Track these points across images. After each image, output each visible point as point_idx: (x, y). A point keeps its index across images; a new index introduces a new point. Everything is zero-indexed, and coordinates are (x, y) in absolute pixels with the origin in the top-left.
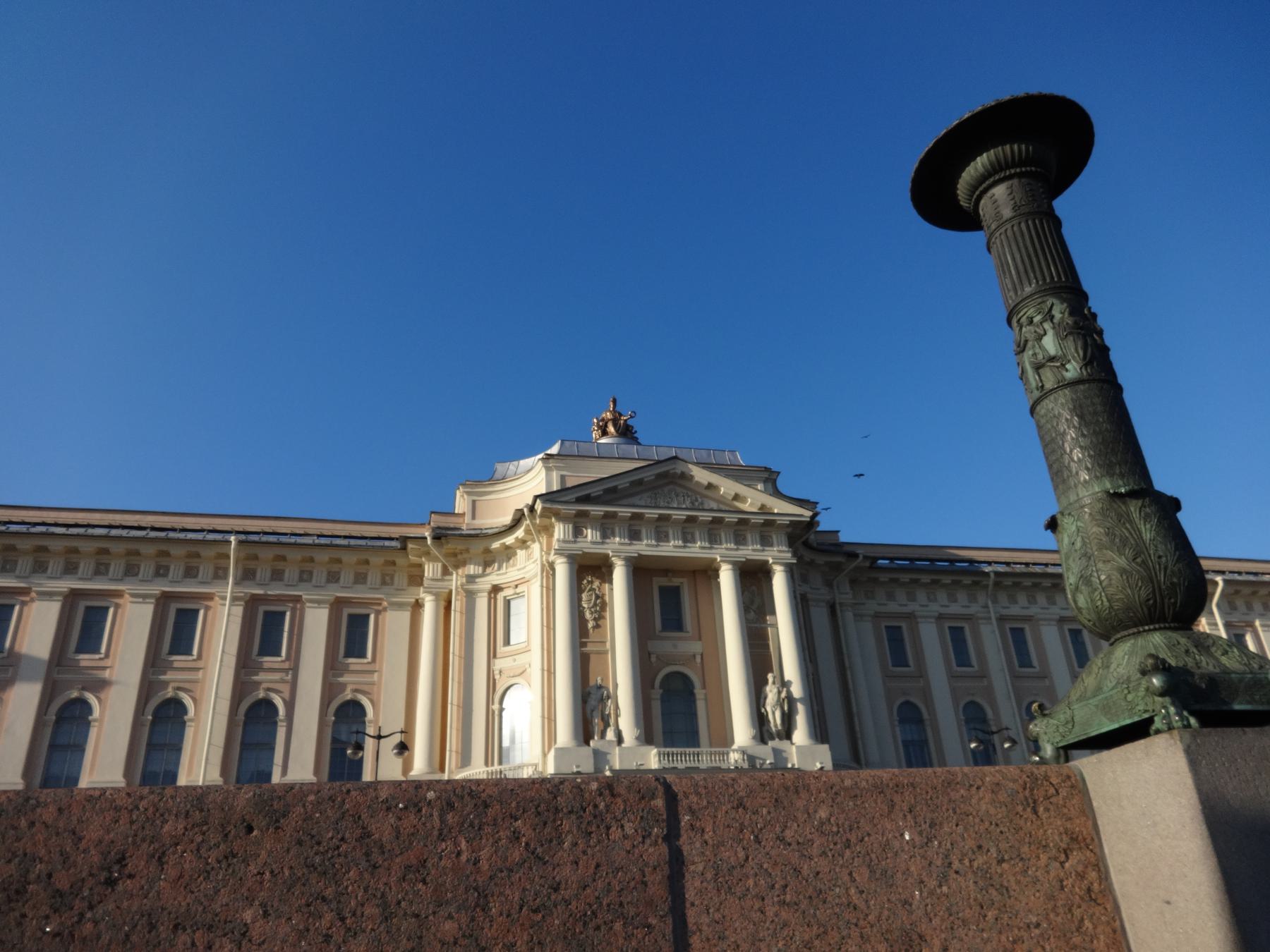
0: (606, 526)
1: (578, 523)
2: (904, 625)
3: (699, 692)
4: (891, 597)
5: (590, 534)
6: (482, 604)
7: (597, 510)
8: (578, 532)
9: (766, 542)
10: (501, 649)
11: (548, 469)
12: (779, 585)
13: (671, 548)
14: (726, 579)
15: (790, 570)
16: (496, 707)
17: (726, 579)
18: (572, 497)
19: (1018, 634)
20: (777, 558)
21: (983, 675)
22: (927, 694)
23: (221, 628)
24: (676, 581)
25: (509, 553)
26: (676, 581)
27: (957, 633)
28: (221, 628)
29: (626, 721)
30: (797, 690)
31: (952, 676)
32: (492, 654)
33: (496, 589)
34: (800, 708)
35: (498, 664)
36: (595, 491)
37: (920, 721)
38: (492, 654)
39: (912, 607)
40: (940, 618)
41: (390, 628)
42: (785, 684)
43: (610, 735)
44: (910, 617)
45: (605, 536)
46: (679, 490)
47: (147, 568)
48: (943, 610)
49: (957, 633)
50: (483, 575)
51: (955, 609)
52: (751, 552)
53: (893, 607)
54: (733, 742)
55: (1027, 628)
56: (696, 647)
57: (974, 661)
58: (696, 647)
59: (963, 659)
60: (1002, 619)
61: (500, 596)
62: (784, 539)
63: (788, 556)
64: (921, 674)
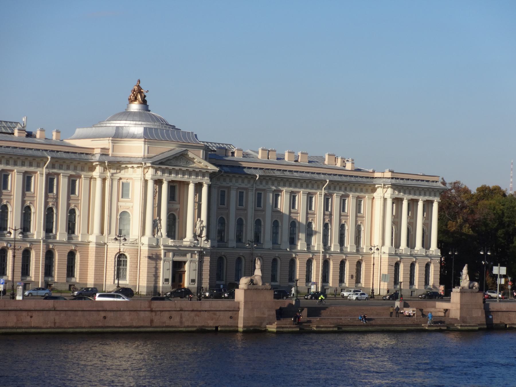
0: (163, 171)
1: (156, 170)
2: (226, 191)
3: (177, 220)
4: (224, 180)
5: (159, 173)
6: (115, 183)
7: (164, 167)
8: (156, 172)
9: (204, 176)
10: (120, 199)
11: (145, 144)
12: (205, 190)
13: (180, 177)
14: (191, 188)
15: (210, 187)
16: (119, 217)
17: (191, 188)
18: (158, 163)
19: (259, 195)
20: (206, 181)
21: (246, 209)
22: (228, 215)
23: (39, 183)
24: (175, 184)
25: (126, 168)
26: (175, 184)
27: (241, 194)
28: (39, 183)
29: (163, 230)
30: (205, 224)
31: (237, 209)
32: (118, 201)
33: (120, 179)
34: (205, 229)
35: (120, 204)
36: (163, 161)
37: (224, 223)
38: (118, 201)
39: (231, 184)
40: (239, 188)
41: (81, 184)
42: (202, 222)
43: (159, 234)
44: (229, 188)
45: (163, 174)
46: (184, 158)
47: (19, 162)
48: (239, 186)
49: (241, 194)
50: (116, 173)
51: (243, 186)
52: (199, 179)
53: (224, 184)
54: (185, 237)
55: (263, 193)
56: (178, 206)
57: (244, 204)
58: (178, 206)
59: (241, 204)
60: (256, 190)
61: (121, 181)
62: (209, 175)
63: (209, 182)
64: (228, 208)
